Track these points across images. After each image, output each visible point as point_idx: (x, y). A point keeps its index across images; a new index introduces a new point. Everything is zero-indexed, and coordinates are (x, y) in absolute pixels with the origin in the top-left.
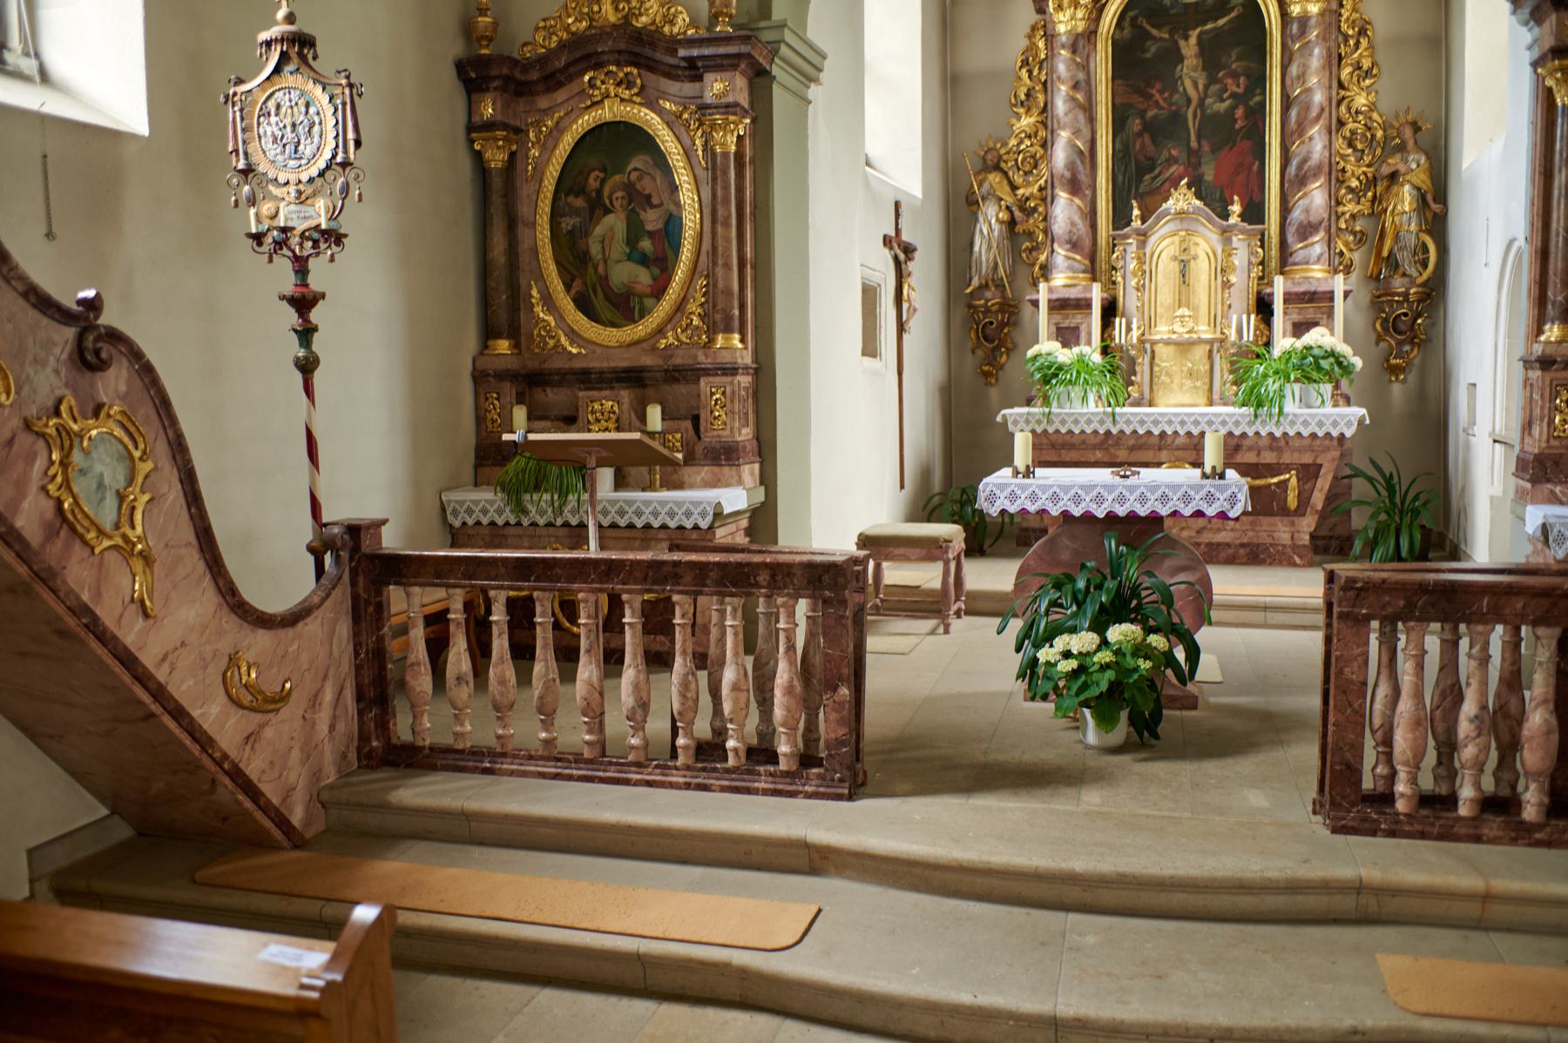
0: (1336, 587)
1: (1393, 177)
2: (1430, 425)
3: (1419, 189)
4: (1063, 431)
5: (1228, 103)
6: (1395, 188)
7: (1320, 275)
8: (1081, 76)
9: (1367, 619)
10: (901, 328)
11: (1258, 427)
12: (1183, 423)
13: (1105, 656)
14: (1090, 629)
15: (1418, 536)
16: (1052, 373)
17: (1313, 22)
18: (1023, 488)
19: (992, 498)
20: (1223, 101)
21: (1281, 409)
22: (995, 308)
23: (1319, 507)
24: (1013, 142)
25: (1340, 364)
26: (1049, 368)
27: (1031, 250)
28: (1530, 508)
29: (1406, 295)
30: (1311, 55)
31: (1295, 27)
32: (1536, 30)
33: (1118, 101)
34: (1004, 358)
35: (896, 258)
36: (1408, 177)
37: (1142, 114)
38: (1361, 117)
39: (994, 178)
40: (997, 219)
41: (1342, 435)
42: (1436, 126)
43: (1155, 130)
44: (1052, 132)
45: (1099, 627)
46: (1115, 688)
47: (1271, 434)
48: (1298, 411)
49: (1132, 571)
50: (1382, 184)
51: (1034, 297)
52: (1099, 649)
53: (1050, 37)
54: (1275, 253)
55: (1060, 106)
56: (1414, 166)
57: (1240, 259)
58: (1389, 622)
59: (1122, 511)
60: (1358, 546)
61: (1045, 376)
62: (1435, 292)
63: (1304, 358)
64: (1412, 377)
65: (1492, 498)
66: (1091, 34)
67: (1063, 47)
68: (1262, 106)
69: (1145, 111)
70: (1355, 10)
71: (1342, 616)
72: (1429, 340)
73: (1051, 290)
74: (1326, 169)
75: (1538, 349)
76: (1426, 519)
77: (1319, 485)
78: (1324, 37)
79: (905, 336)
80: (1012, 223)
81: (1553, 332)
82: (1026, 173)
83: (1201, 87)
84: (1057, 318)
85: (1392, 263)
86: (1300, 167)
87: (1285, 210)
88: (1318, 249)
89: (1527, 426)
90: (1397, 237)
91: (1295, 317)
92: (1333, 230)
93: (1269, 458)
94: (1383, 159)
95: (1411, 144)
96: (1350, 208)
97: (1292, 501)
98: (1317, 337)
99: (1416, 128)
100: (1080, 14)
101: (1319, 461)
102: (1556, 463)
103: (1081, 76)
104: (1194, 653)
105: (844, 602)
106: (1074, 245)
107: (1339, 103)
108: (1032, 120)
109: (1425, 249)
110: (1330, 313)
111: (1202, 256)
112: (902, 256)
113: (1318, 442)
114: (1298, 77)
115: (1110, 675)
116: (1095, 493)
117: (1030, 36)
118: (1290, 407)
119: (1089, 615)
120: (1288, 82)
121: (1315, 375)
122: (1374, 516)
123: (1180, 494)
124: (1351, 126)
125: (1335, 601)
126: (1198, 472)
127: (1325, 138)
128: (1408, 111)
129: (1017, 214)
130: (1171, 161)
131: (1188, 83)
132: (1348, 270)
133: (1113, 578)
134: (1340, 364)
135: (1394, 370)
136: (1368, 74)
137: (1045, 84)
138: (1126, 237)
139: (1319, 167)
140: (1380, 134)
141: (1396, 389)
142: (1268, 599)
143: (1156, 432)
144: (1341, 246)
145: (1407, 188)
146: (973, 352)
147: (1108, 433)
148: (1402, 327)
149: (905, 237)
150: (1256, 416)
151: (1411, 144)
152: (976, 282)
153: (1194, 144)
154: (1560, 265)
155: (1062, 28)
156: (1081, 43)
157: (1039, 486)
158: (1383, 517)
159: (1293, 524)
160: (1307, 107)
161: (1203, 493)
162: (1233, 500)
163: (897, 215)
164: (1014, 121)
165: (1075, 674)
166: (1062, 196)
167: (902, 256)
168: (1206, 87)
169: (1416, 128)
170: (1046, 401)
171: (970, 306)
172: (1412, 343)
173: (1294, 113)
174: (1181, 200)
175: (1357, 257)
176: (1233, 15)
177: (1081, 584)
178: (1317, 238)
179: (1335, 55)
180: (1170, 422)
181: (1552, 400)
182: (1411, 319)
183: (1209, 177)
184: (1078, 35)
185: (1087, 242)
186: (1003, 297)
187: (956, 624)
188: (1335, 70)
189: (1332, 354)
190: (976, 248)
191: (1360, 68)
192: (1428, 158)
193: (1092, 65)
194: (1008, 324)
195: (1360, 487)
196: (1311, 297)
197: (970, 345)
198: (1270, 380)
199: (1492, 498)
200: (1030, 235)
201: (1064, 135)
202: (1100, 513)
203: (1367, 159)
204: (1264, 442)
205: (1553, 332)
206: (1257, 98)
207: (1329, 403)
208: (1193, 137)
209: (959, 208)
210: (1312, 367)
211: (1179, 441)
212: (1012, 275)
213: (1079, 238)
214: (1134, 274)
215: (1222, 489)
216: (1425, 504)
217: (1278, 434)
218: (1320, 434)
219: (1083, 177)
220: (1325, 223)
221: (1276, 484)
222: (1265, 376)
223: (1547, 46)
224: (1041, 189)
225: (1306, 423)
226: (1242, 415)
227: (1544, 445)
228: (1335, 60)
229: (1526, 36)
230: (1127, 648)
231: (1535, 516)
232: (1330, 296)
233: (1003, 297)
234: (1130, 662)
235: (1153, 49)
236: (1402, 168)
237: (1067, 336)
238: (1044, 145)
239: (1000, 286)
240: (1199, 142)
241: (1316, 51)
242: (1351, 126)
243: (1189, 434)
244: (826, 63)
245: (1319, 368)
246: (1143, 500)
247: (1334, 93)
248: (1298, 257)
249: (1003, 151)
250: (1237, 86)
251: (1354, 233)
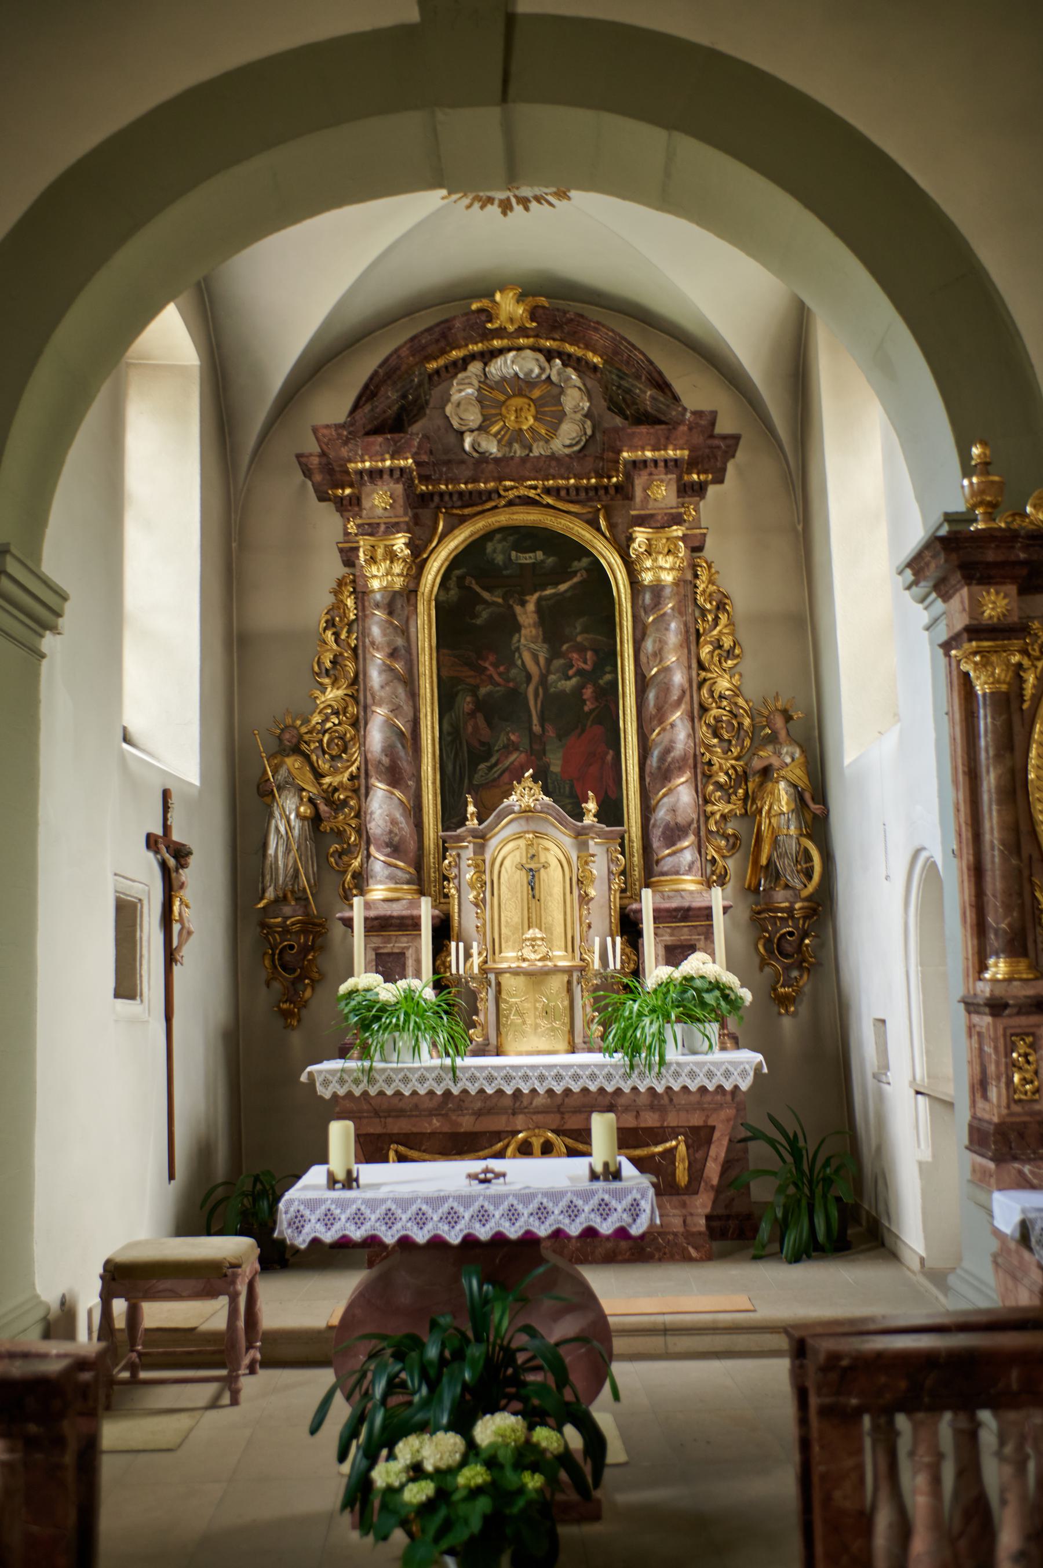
0: (811, 1365)
1: (766, 772)
2: (821, 1063)
3: (795, 786)
4: (389, 1092)
5: (574, 681)
6: (770, 785)
7: (692, 887)
8: (400, 642)
9: (857, 1413)
10: (170, 957)
11: (635, 1080)
12: (542, 1078)
13: (474, 1475)
14: (450, 1428)
15: (834, 1213)
16: (373, 1015)
17: (668, 592)
18: (343, 1204)
19: (298, 1222)
20: (569, 678)
21: (662, 1057)
22: (296, 928)
23: (715, 1181)
24: (316, 719)
25: (726, 997)
26: (369, 1008)
27: (340, 854)
28: (997, 1196)
29: (790, 910)
30: (667, 629)
31: (648, 597)
32: (939, 606)
33: (445, 674)
34: (308, 993)
35: (164, 865)
36: (783, 773)
37: (474, 690)
38: (725, 703)
39: (293, 763)
40: (298, 815)
41: (736, 1087)
42: (808, 715)
43: (486, 708)
44: (365, 708)
45: (462, 1424)
46: (493, 1521)
47: (651, 1090)
48: (682, 1059)
49: (501, 1319)
51: (347, 914)
52: (464, 1463)
53: (361, 594)
54: (637, 859)
55: (375, 677)
56: (788, 760)
57: (599, 867)
58: (888, 1412)
59: (484, 1233)
60: (765, 1229)
61: (363, 1020)
62: (822, 907)
63: (684, 992)
64: (804, 1008)
65: (920, 1164)
66: (410, 593)
67: (377, 606)
68: (614, 684)
69: (477, 687)
70: (711, 582)
71: (825, 1412)
72: (819, 964)
73: (367, 905)
74: (691, 761)
75: (984, 990)
76: (842, 1189)
77: (713, 1151)
78: (680, 610)
79: (176, 969)
80: (315, 820)
81: (999, 968)
82: (333, 758)
83: (542, 661)
84: (376, 941)
85: (772, 872)
86: (662, 758)
87: (647, 809)
88: (688, 856)
89: (980, 1086)
90: (775, 843)
91: (668, 939)
92: (703, 833)
93: (650, 1120)
94: (753, 752)
95: (783, 734)
96: (720, 807)
97: (682, 1175)
98: (696, 964)
99: (788, 718)
100: (397, 568)
101: (710, 1123)
102: (1021, 1135)
103: (400, 642)
104: (595, 1441)
105: (59, 1442)
106: (395, 849)
107: (701, 685)
108: (340, 693)
109: (809, 858)
110: (708, 933)
111: (554, 863)
112: (172, 862)
113: (708, 1098)
114: (655, 654)
115: (483, 1504)
116: (445, 1208)
117: (337, 592)
118: (673, 1055)
119: (447, 1403)
120: (643, 659)
121: (699, 1013)
122: (781, 1190)
123: (563, 1204)
124: (715, 712)
125: (810, 1384)
126: (579, 1166)
127: (688, 725)
128: (776, 698)
129: (323, 808)
130: (511, 747)
131: (527, 657)
132: (722, 882)
133: (479, 1339)
134: (726, 997)
135: (783, 1001)
136: (730, 654)
137: (355, 650)
138: (460, 839)
139: (684, 758)
140: (747, 722)
141: (787, 1022)
142: (668, 1318)
143: (509, 1091)
144: (712, 852)
145: (782, 785)
146: (268, 984)
147: (448, 1093)
148: (789, 949)
149: (176, 837)
150: (632, 1067)
151: (783, 734)
152: (270, 894)
153: (537, 728)
154: (999, 885)
155: (375, 584)
156: (399, 603)
157: (366, 1202)
158: (791, 1190)
159: (684, 1205)
160: (666, 689)
161: (594, 1202)
162: (634, 1209)
163: (166, 808)
164: (317, 693)
165: (428, 1507)
166: (380, 790)
167: (172, 862)
168: (549, 661)
169: (788, 718)
170: (365, 1052)
171: (263, 925)
172: (800, 967)
173: (651, 695)
174: (526, 795)
175: (731, 864)
176: (575, 580)
177: (432, 1352)
178: (686, 844)
179: (692, 630)
180: (526, 1078)
181: (1008, 1054)
182: (798, 938)
183: (556, 768)
184: (395, 592)
185: (412, 845)
186: (307, 914)
187: (248, 1384)
188: (693, 647)
189: (716, 986)
190: (271, 851)
191: (720, 647)
192: (803, 751)
193: (412, 630)
194: (312, 948)
195: (758, 1150)
196: (684, 914)
197: (263, 975)
198: (647, 1021)
199: (920, 1164)
200: (340, 835)
201: (380, 714)
202: (454, 1238)
203: (735, 751)
204: (643, 1100)
205: (999, 968)
206: (608, 677)
207: (716, 1048)
208: (535, 720)
209: (246, 798)
210: (693, 1003)
211: (538, 1102)
212: (317, 885)
213: (402, 840)
214: (472, 886)
215: (618, 1195)
216: (837, 1171)
217: (660, 1090)
218: (711, 1088)
219: (405, 765)
220: (695, 825)
221: (661, 1154)
222: (640, 1015)
223: (959, 626)
224: (352, 778)
225: (692, 1074)
226: (615, 1066)
227: (1004, 1111)
228: (693, 637)
229: (922, 615)
230: (505, 1456)
231: (1008, 1209)
232: (707, 913)
233: (307, 914)
234: (511, 1478)
235: (485, 615)
236: (775, 762)
237: (390, 966)
238: (355, 724)
239: (302, 899)
240: (542, 726)
241: (673, 625)
242: (715, 712)
243: (550, 1092)
244: (68, 607)
245: (703, 1004)
246: (512, 1215)
247: (694, 674)
248: (667, 865)
249: (304, 730)
250: (587, 662)
251: (726, 837)
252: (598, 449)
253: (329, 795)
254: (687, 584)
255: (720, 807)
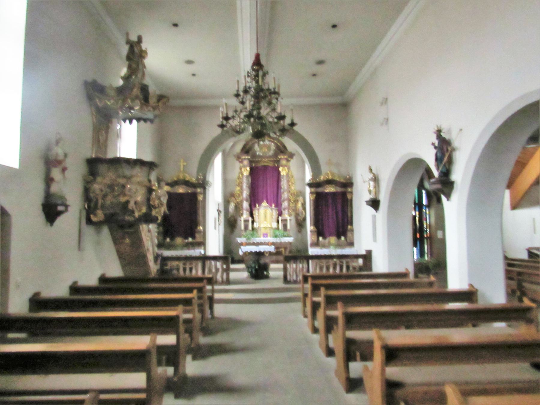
10: (219, 224)
39: (233, 198)
50: (296, 201)
106: (247, 210)
174: (265, 204)
209: (227, 202)
228: (288, 181)
252: (276, 155)
253: (238, 203)
254: (287, 175)
255: (291, 205)
